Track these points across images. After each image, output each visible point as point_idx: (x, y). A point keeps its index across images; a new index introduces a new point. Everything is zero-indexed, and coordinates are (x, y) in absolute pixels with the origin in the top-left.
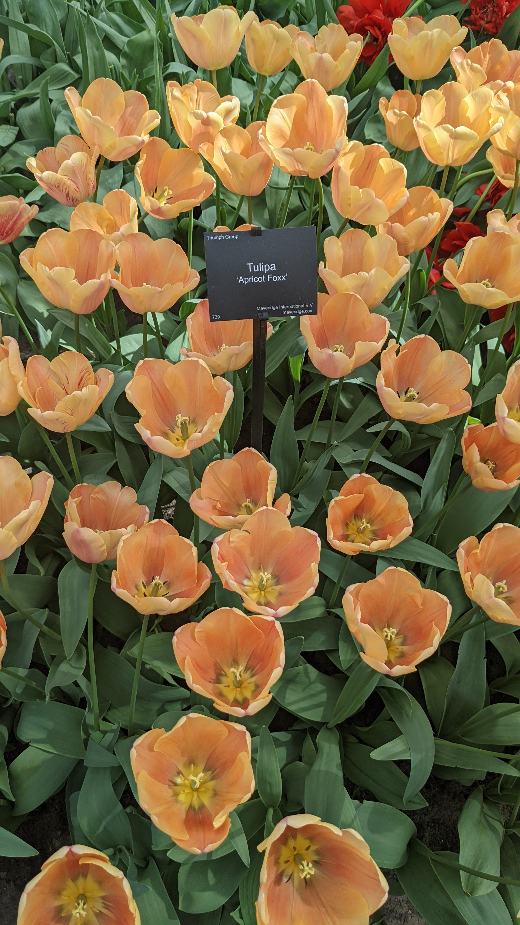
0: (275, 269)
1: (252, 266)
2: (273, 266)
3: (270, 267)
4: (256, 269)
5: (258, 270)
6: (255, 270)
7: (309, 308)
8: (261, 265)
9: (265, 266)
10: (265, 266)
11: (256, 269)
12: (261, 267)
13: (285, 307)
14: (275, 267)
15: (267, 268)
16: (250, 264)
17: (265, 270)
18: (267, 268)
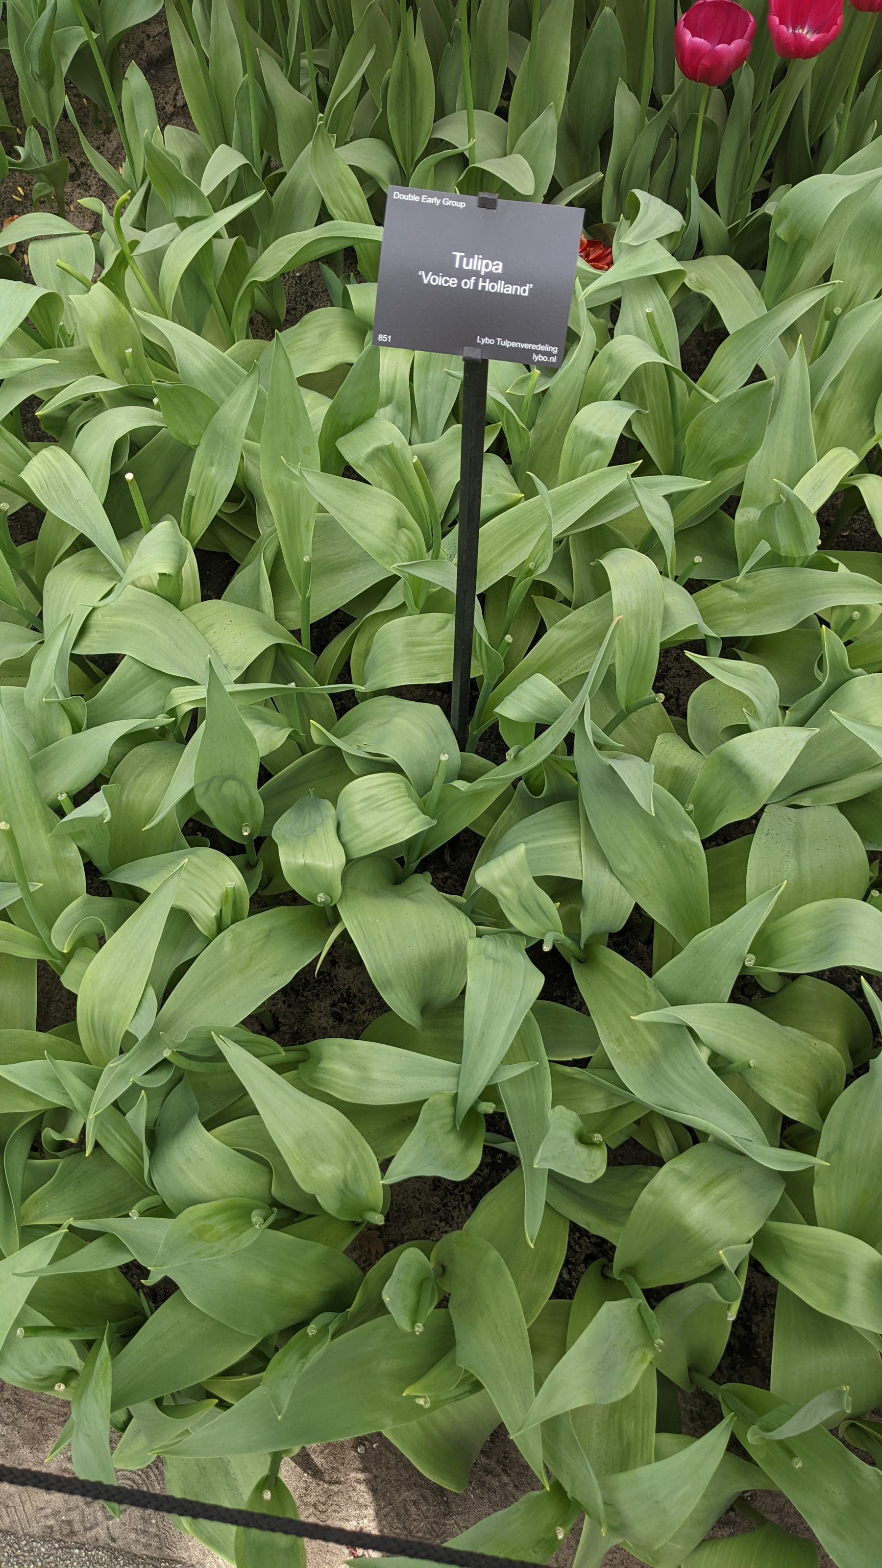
0: (500, 271)
1: (462, 258)
4: (467, 265)
8: (479, 258)
11: (467, 265)
12: (477, 263)
15: (487, 266)
16: (458, 255)
18: (487, 266)
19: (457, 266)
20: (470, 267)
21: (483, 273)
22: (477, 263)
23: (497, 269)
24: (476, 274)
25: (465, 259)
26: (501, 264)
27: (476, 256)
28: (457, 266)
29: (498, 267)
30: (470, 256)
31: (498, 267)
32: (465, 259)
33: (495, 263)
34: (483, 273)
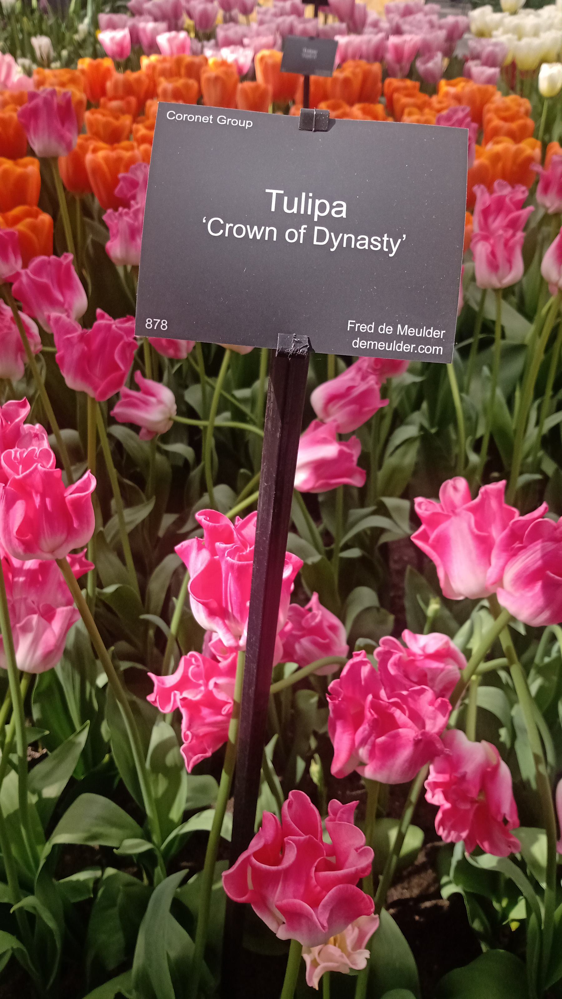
0: (344, 215)
1: (280, 198)
2: (341, 206)
3: (332, 207)
4: (290, 206)
5: (295, 210)
8: (307, 198)
9: (318, 202)
10: (318, 202)
11: (290, 206)
13: (364, 328)
14: (344, 209)
15: (322, 208)
16: (275, 192)
17: (317, 213)
18: (322, 208)
20: (295, 210)
21: (316, 219)
24: (308, 219)
25: (286, 199)
27: (304, 194)
28: (273, 209)
30: (292, 194)
32: (286, 199)
33: (334, 204)
34: (316, 219)
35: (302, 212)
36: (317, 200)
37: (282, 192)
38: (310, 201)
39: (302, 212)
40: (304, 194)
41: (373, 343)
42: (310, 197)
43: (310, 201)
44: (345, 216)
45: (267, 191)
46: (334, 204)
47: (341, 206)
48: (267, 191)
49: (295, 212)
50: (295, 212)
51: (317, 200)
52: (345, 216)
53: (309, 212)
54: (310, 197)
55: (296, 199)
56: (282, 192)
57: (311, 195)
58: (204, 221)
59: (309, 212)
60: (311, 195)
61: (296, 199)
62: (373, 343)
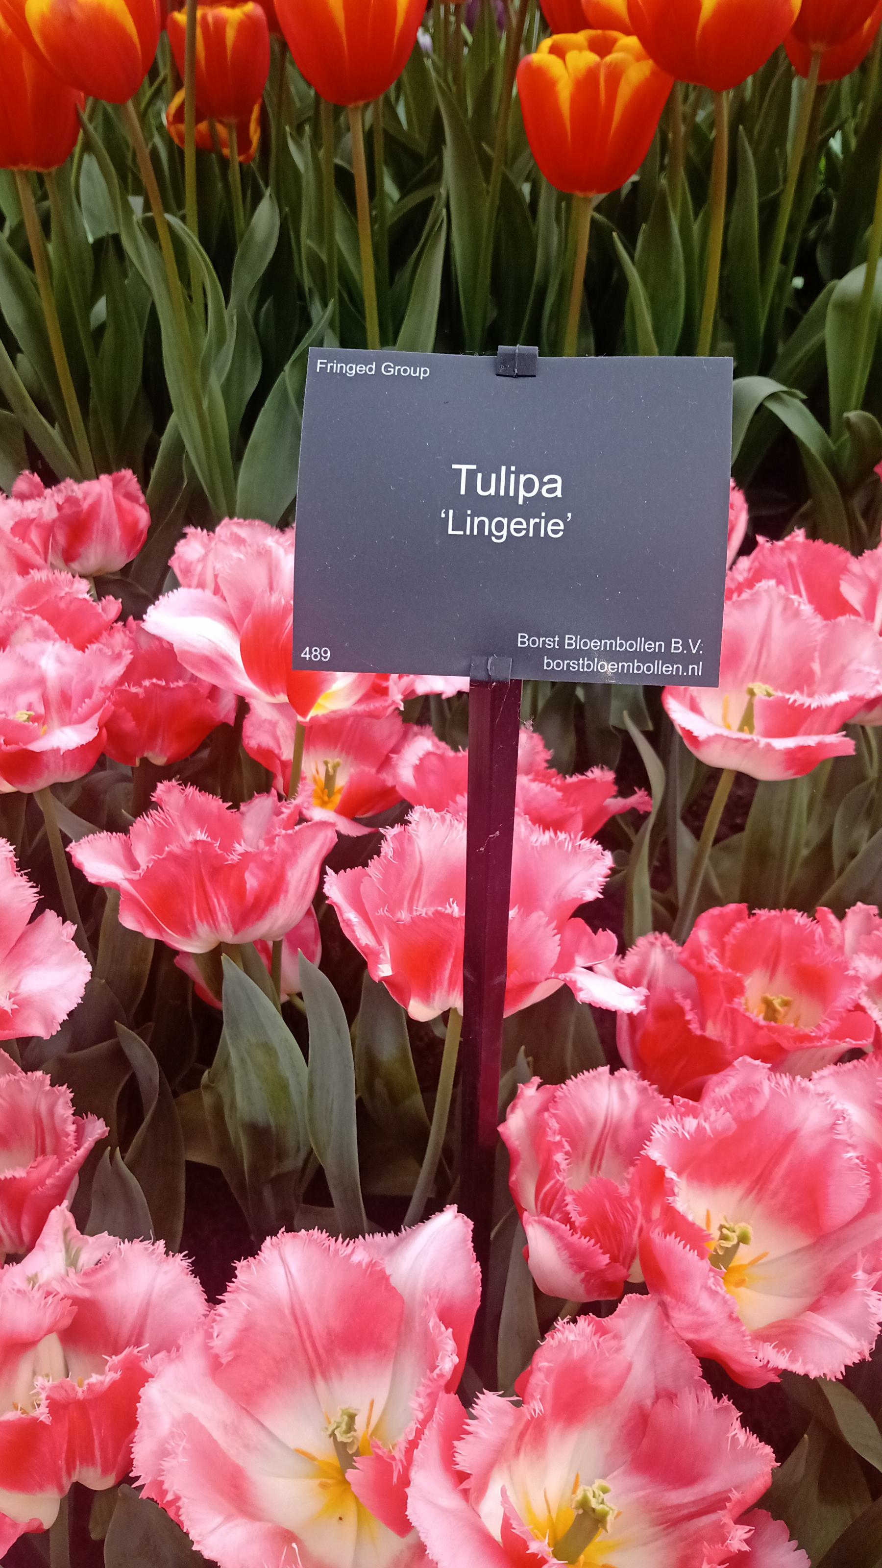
0: (559, 493)
1: (471, 475)
2: (555, 481)
3: (542, 484)
4: (486, 487)
5: (492, 491)
6: (480, 491)
7: (686, 659)
9: (523, 478)
10: (523, 478)
11: (486, 487)
12: (507, 483)
14: (559, 485)
16: (464, 468)
17: (522, 493)
19: (463, 492)
21: (521, 502)
22: (507, 483)
23: (549, 491)
25: (480, 476)
26: (559, 479)
27: (504, 468)
28: (463, 492)
29: (554, 486)
30: (488, 468)
31: (554, 486)
32: (480, 476)
33: (546, 479)
34: (521, 502)
35: (502, 493)
36: (522, 476)
37: (474, 467)
38: (513, 477)
39: (502, 493)
40: (504, 468)
41: (626, 665)
42: (513, 472)
43: (513, 477)
44: (560, 496)
45: (454, 466)
46: (546, 479)
47: (555, 481)
48: (454, 466)
49: (493, 494)
50: (493, 494)
51: (522, 476)
52: (560, 496)
53: (512, 494)
54: (513, 472)
55: (494, 476)
56: (474, 467)
57: (513, 468)
58: (443, 515)
59: (512, 494)
60: (513, 468)
61: (494, 476)
62: (626, 665)
